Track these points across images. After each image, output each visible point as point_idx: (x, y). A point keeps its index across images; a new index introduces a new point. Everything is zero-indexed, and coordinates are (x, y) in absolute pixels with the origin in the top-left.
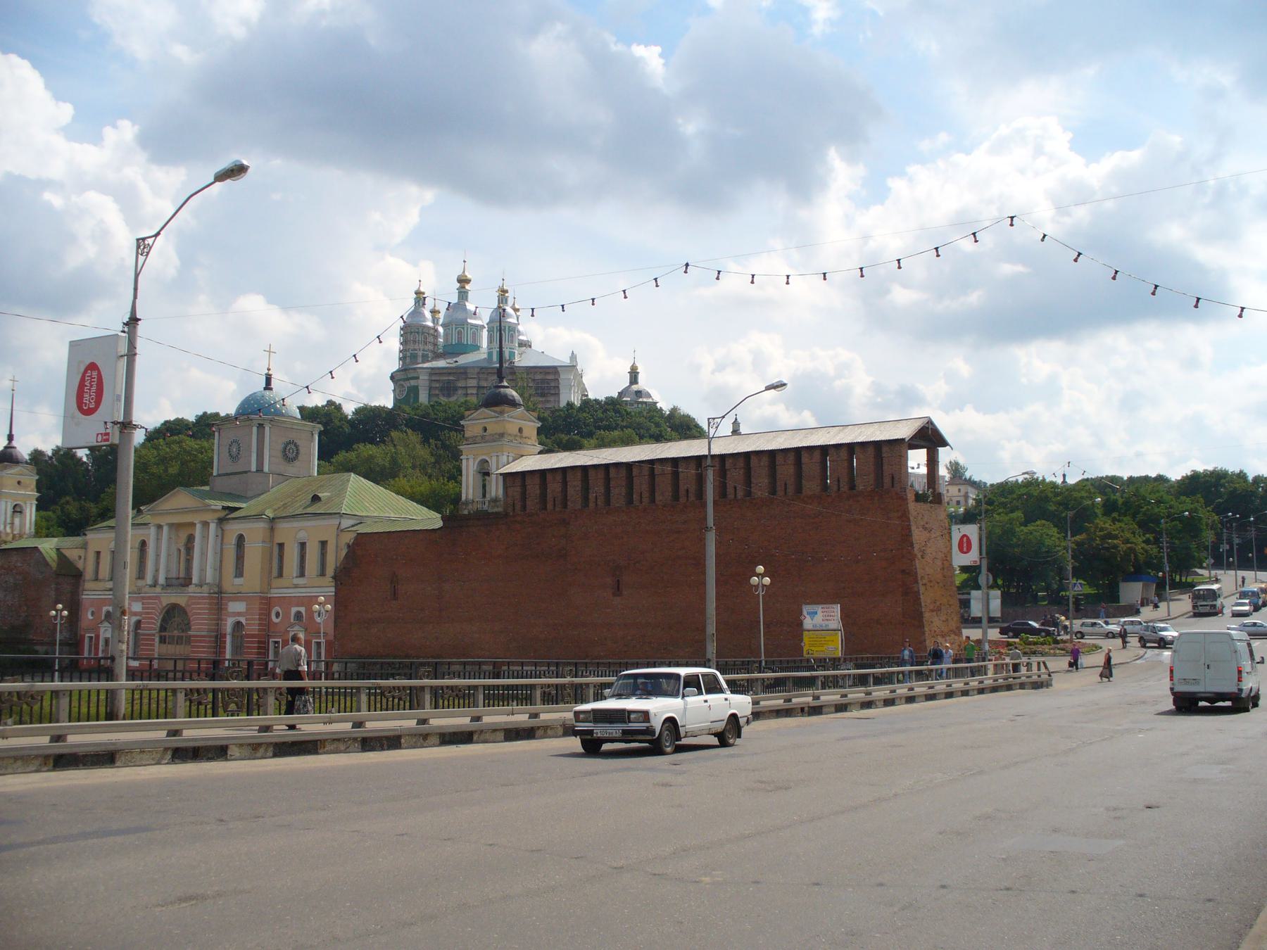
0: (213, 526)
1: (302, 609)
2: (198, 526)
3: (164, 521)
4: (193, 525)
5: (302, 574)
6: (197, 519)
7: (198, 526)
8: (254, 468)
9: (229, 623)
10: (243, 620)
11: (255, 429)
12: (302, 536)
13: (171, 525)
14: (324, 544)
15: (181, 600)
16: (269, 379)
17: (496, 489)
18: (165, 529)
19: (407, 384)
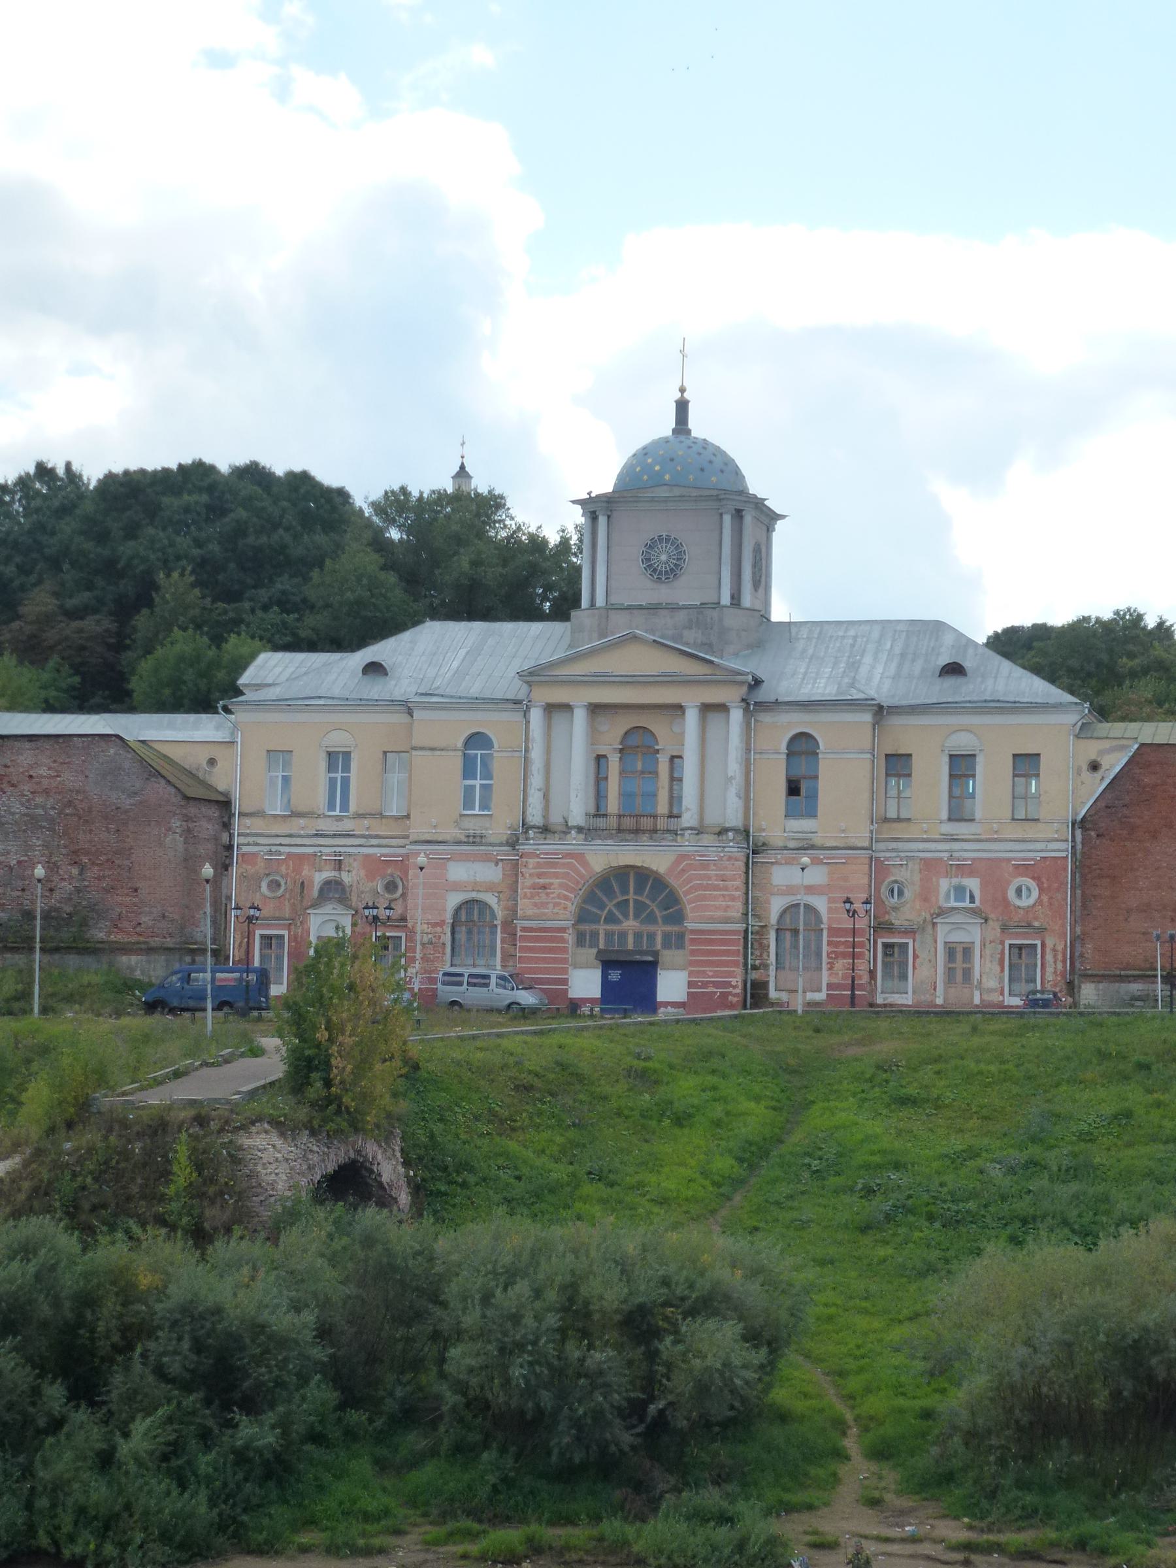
0: (736, 715)
1: (973, 884)
2: (692, 717)
3: (581, 698)
4: (679, 708)
5: (957, 815)
6: (692, 699)
7: (692, 717)
8: (726, 600)
9: (776, 905)
10: (821, 904)
11: (727, 519)
12: (963, 742)
13: (595, 709)
15: (655, 857)
16: (682, 407)
18: (580, 716)
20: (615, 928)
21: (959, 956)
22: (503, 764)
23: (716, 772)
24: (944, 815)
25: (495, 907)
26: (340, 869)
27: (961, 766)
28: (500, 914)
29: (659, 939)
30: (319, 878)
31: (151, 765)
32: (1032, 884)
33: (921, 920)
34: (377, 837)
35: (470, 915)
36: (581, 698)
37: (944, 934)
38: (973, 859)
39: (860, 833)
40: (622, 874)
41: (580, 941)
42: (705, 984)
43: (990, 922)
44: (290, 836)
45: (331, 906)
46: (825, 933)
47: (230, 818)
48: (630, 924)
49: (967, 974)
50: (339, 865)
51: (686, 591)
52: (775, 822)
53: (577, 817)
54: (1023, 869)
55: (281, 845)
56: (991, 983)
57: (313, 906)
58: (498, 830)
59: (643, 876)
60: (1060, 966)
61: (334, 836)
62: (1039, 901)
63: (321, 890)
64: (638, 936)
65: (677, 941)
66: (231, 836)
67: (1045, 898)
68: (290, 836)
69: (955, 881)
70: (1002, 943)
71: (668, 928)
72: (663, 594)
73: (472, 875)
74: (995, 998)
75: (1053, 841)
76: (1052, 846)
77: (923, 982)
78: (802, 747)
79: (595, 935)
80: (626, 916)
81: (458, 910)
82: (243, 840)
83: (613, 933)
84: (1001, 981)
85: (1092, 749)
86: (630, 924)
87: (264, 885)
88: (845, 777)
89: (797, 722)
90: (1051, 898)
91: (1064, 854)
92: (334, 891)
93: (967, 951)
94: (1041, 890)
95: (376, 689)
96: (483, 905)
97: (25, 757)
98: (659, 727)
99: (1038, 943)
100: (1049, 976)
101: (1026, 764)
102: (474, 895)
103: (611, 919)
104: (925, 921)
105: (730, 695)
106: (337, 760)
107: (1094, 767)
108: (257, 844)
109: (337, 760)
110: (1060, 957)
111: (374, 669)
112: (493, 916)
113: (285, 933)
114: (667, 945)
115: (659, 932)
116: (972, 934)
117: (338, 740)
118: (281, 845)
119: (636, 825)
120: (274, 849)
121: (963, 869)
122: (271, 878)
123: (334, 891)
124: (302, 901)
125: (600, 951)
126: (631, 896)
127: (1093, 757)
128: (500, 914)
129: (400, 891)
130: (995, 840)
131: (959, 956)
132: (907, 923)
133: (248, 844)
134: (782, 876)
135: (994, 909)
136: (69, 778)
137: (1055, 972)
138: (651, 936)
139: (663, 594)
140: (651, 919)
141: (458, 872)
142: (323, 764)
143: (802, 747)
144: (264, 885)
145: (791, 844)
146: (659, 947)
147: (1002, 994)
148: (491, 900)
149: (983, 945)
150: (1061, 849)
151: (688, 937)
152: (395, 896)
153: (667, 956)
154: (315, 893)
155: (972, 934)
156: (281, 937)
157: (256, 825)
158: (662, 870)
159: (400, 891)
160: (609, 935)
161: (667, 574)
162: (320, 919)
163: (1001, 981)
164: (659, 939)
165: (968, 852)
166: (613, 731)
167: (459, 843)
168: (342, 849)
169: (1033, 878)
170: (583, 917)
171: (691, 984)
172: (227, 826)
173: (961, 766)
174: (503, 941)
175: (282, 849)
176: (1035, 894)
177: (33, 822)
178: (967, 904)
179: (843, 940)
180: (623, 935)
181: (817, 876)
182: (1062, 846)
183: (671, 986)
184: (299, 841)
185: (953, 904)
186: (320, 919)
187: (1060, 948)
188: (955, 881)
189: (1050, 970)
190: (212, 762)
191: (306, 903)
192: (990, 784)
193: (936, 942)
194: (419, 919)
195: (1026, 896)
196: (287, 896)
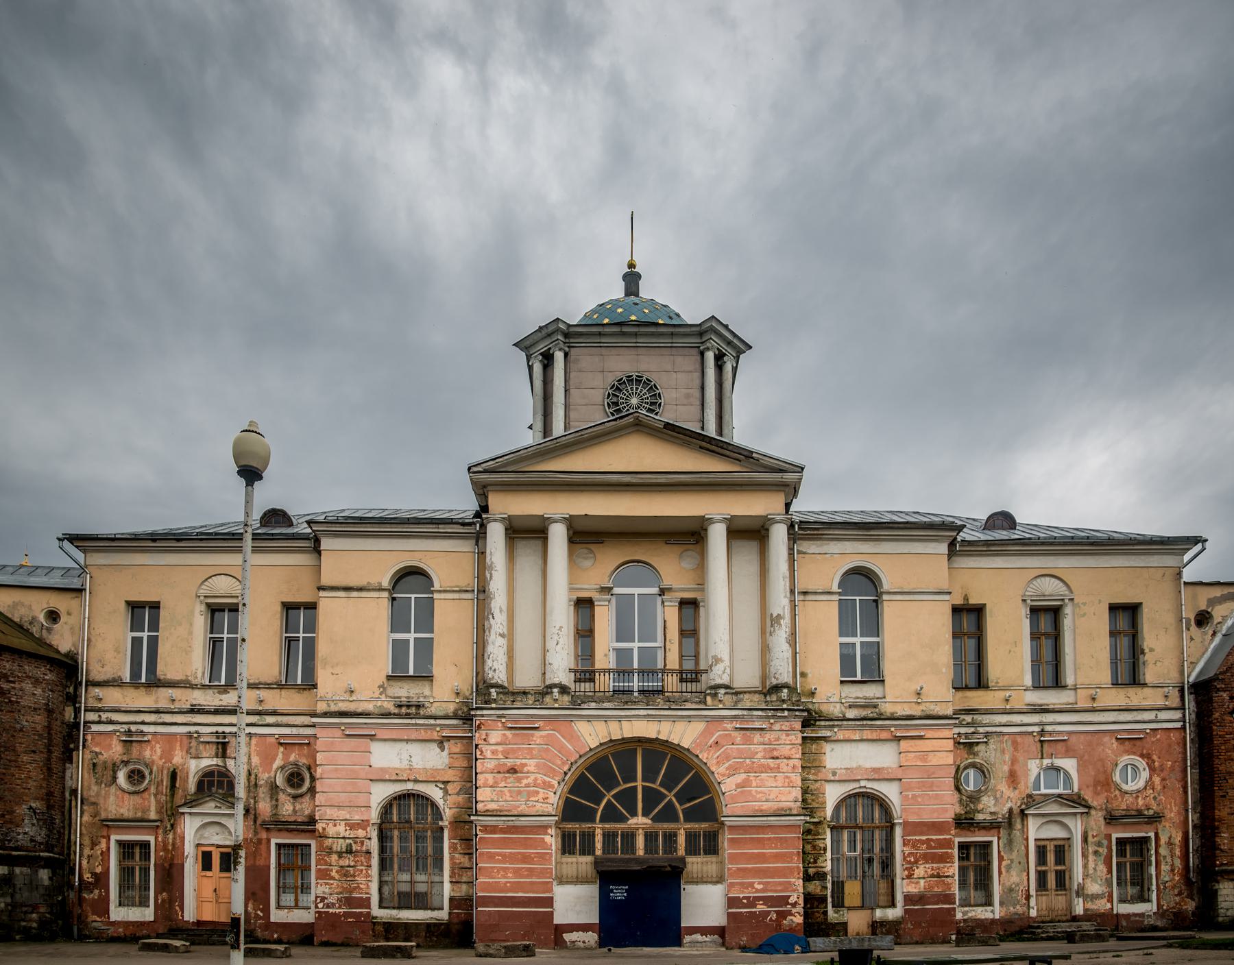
9: (832, 795)
20: (620, 827)
21: (1051, 857)
22: (451, 617)
24: (1028, 681)
25: (440, 803)
26: (224, 756)
27: (1047, 619)
28: (448, 814)
29: (681, 840)
30: (195, 767)
32: (1142, 763)
33: (1005, 810)
34: (274, 713)
35: (406, 816)
38: (1070, 733)
41: (568, 845)
42: (752, 902)
43: (1093, 812)
44: (157, 712)
45: (212, 804)
46: (898, 832)
47: (76, 689)
48: (639, 821)
49: (1062, 880)
50: (222, 747)
54: (1131, 742)
55: (143, 723)
57: (190, 803)
60: (1178, 863)
61: (217, 712)
62: (1149, 784)
63: (200, 785)
64: (650, 837)
65: (709, 844)
66: (77, 711)
67: (1157, 780)
68: (157, 712)
69: (1046, 762)
70: (1109, 837)
71: (695, 826)
74: (1102, 905)
76: (1163, 715)
79: (588, 838)
80: (634, 814)
81: (386, 809)
82: (92, 716)
83: (615, 835)
84: (1110, 884)
86: (639, 821)
87: (121, 777)
90: (1163, 779)
91: (1179, 725)
92: (216, 785)
93: (1062, 851)
94: (1152, 769)
96: (423, 801)
99: (1152, 835)
100: (1165, 877)
102: (410, 786)
103: (611, 815)
104: (1011, 811)
107: (1203, 619)
108: (111, 722)
109: (222, 612)
110: (1178, 852)
112: (438, 814)
113: (151, 839)
114: (692, 850)
115: (682, 832)
117: (223, 586)
118: (143, 723)
120: (133, 728)
121: (1063, 745)
122: (131, 767)
123: (216, 785)
124: (173, 795)
125: (597, 863)
126: (639, 784)
127: (1203, 606)
128: (448, 814)
129: (307, 784)
130: (1093, 710)
131: (1051, 857)
132: (989, 817)
133: (99, 722)
137: (1172, 870)
138: (671, 838)
140: (668, 814)
142: (200, 621)
144: (121, 777)
145: (851, 714)
146: (681, 852)
147: (1111, 900)
148: (436, 794)
149: (1085, 840)
151: (725, 839)
152: (300, 791)
153: (695, 864)
154: (192, 787)
156: (145, 845)
157: (112, 697)
158: (685, 744)
159: (307, 784)
160: (609, 837)
162: (198, 822)
163: (1110, 884)
164: (681, 840)
165: (1060, 724)
167: (387, 715)
168: (227, 729)
169: (1142, 756)
170: (571, 811)
171: (732, 902)
172: (73, 699)
174: (453, 848)
175: (145, 728)
176: (1145, 775)
178: (1060, 791)
179: (924, 838)
180: (629, 837)
181: (882, 756)
182: (1177, 715)
183: (704, 904)
184: (168, 718)
185: (1043, 791)
186: (198, 822)
187: (1178, 838)
188: (1046, 762)
189: (1165, 868)
190: (53, 616)
191: (179, 800)
193: (1027, 839)
195: (1134, 779)
196: (153, 790)
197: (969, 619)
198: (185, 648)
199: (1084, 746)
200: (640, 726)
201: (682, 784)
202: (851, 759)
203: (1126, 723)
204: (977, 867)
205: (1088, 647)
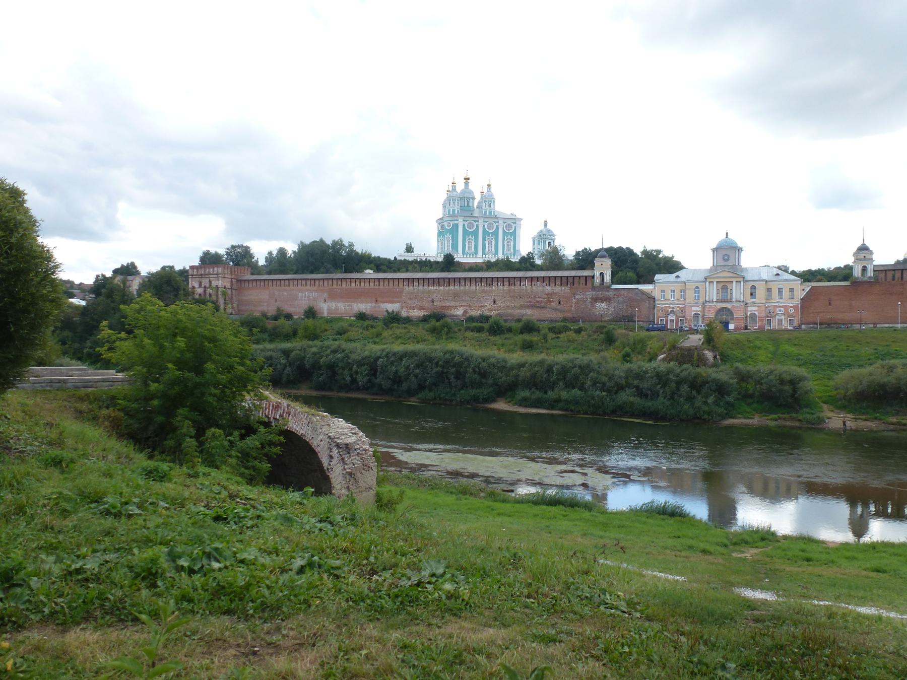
3: (715, 280)
6: (734, 280)
9: (749, 313)
12: (781, 286)
14: (792, 290)
15: (729, 306)
17: (870, 273)
19: (452, 223)
23: (738, 292)
27: (780, 291)
31: (642, 292)
36: (715, 280)
37: (777, 317)
39: (764, 301)
40: (722, 309)
51: (730, 263)
52: (749, 300)
53: (715, 299)
56: (786, 325)
58: (701, 301)
59: (726, 309)
65: (732, 319)
72: (726, 263)
73: (697, 309)
75: (796, 302)
77: (774, 325)
78: (753, 287)
85: (803, 287)
88: (761, 293)
89: (753, 284)
92: (672, 312)
95: (679, 280)
97: (623, 292)
98: (729, 286)
101: (792, 290)
105: (741, 279)
106: (673, 291)
109: (673, 291)
111: (678, 277)
116: (783, 317)
117: (673, 288)
119: (724, 301)
134: (750, 308)
135: (786, 313)
136: (630, 295)
139: (726, 263)
141: (694, 309)
143: (753, 287)
150: (798, 303)
155: (783, 317)
161: (728, 260)
165: (782, 304)
166: (720, 286)
173: (780, 291)
177: (624, 302)
192: (786, 293)
194: (688, 316)
197: (769, 290)
198: (668, 295)
199: (785, 307)
200: (724, 305)
201: (729, 312)
202: (751, 309)
203: (791, 304)
204: (769, 322)
205: (786, 293)
